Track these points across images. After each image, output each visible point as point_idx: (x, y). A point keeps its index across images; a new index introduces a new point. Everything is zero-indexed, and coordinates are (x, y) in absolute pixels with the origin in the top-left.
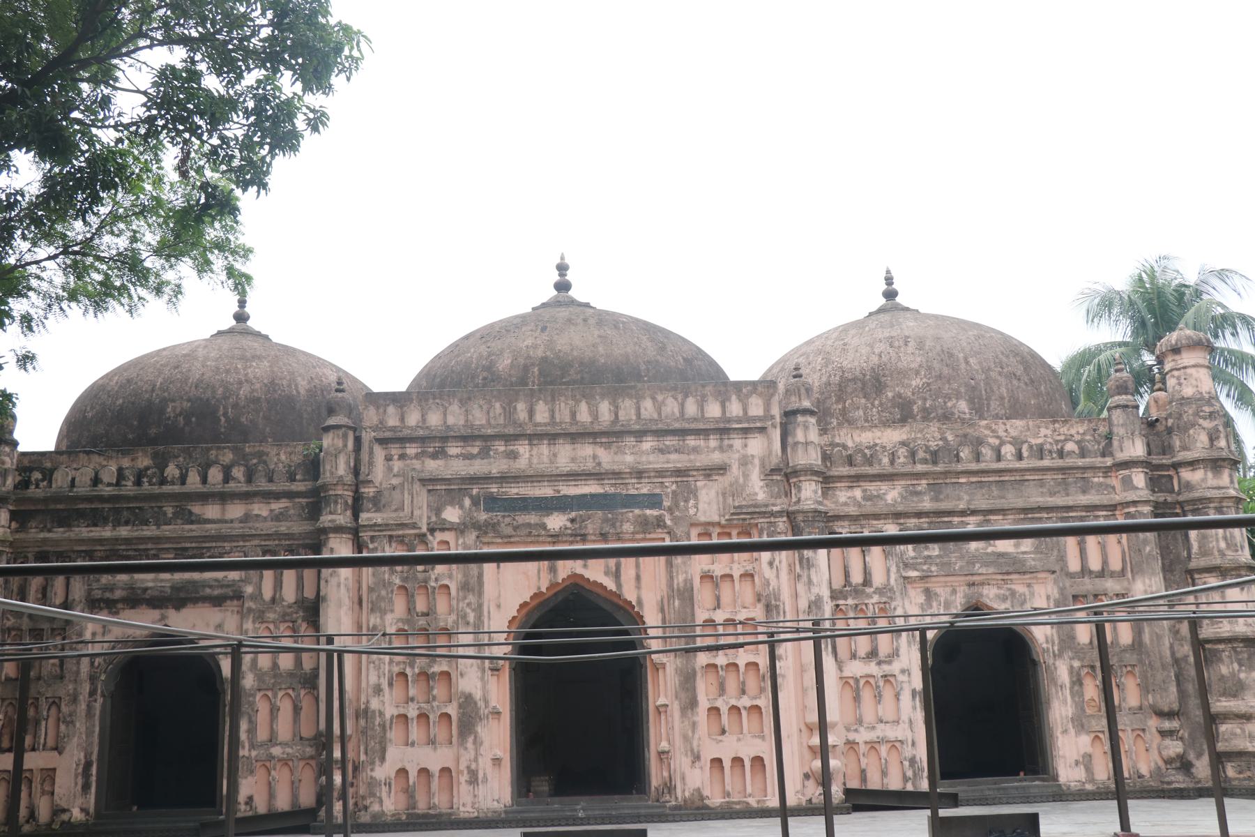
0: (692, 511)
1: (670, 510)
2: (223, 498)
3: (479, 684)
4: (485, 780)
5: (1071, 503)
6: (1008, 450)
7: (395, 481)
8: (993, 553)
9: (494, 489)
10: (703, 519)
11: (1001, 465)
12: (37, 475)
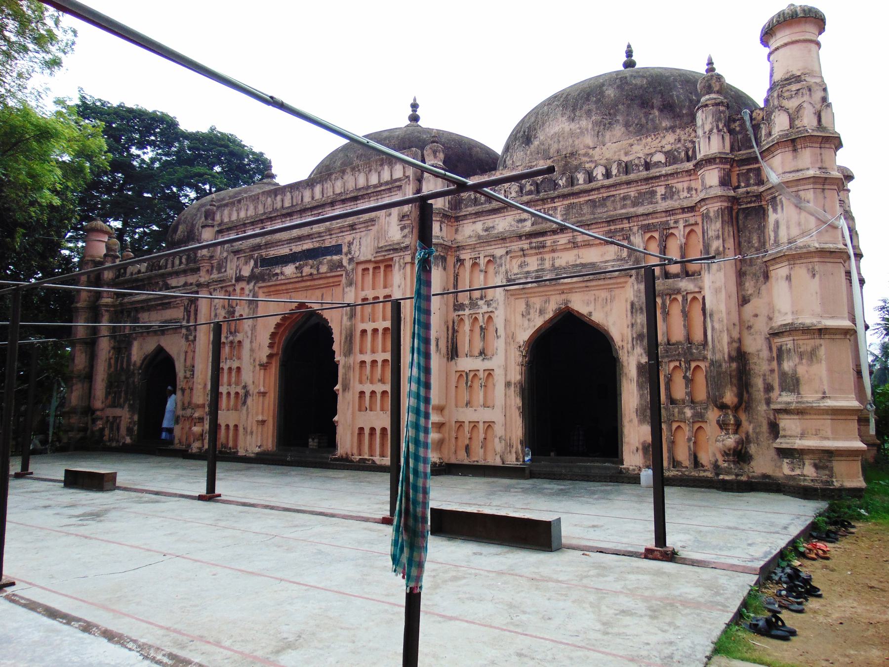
0: (357, 254)
1: (346, 255)
2: (177, 274)
3: (251, 374)
4: (252, 433)
5: (651, 210)
6: (599, 172)
7: (225, 254)
8: (583, 265)
9: (264, 253)
10: (362, 259)
11: (593, 185)
12: (122, 271)
